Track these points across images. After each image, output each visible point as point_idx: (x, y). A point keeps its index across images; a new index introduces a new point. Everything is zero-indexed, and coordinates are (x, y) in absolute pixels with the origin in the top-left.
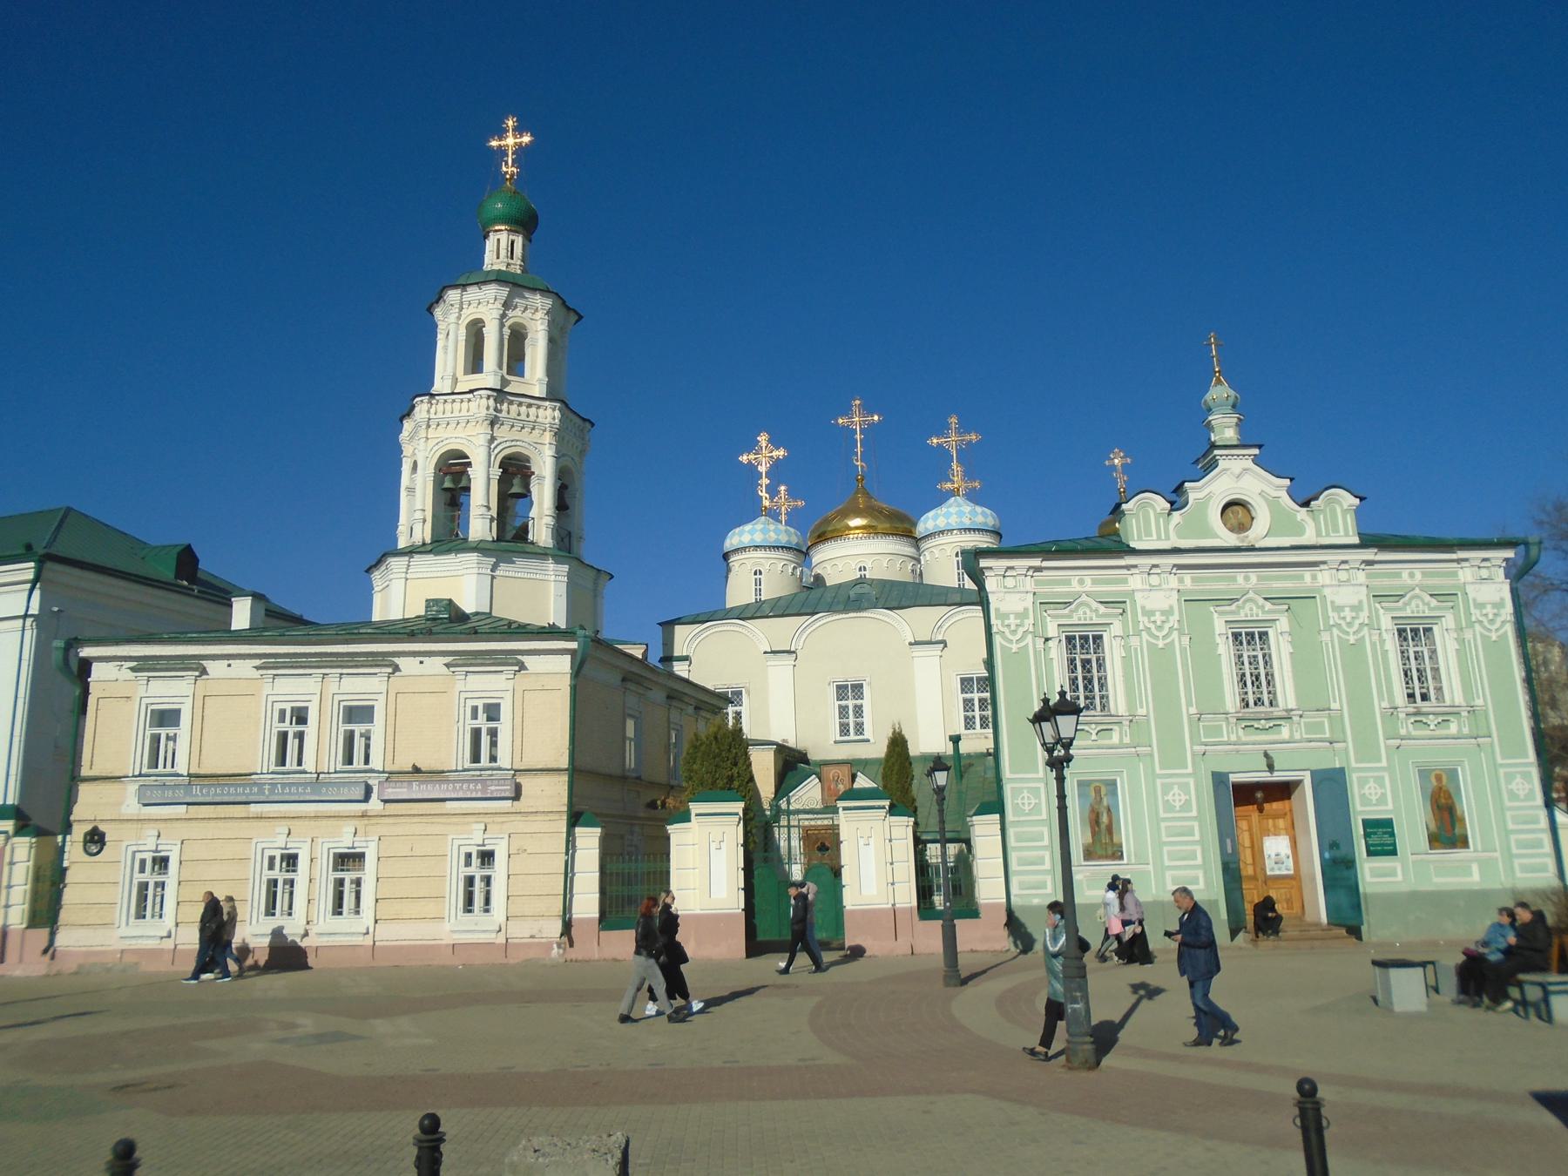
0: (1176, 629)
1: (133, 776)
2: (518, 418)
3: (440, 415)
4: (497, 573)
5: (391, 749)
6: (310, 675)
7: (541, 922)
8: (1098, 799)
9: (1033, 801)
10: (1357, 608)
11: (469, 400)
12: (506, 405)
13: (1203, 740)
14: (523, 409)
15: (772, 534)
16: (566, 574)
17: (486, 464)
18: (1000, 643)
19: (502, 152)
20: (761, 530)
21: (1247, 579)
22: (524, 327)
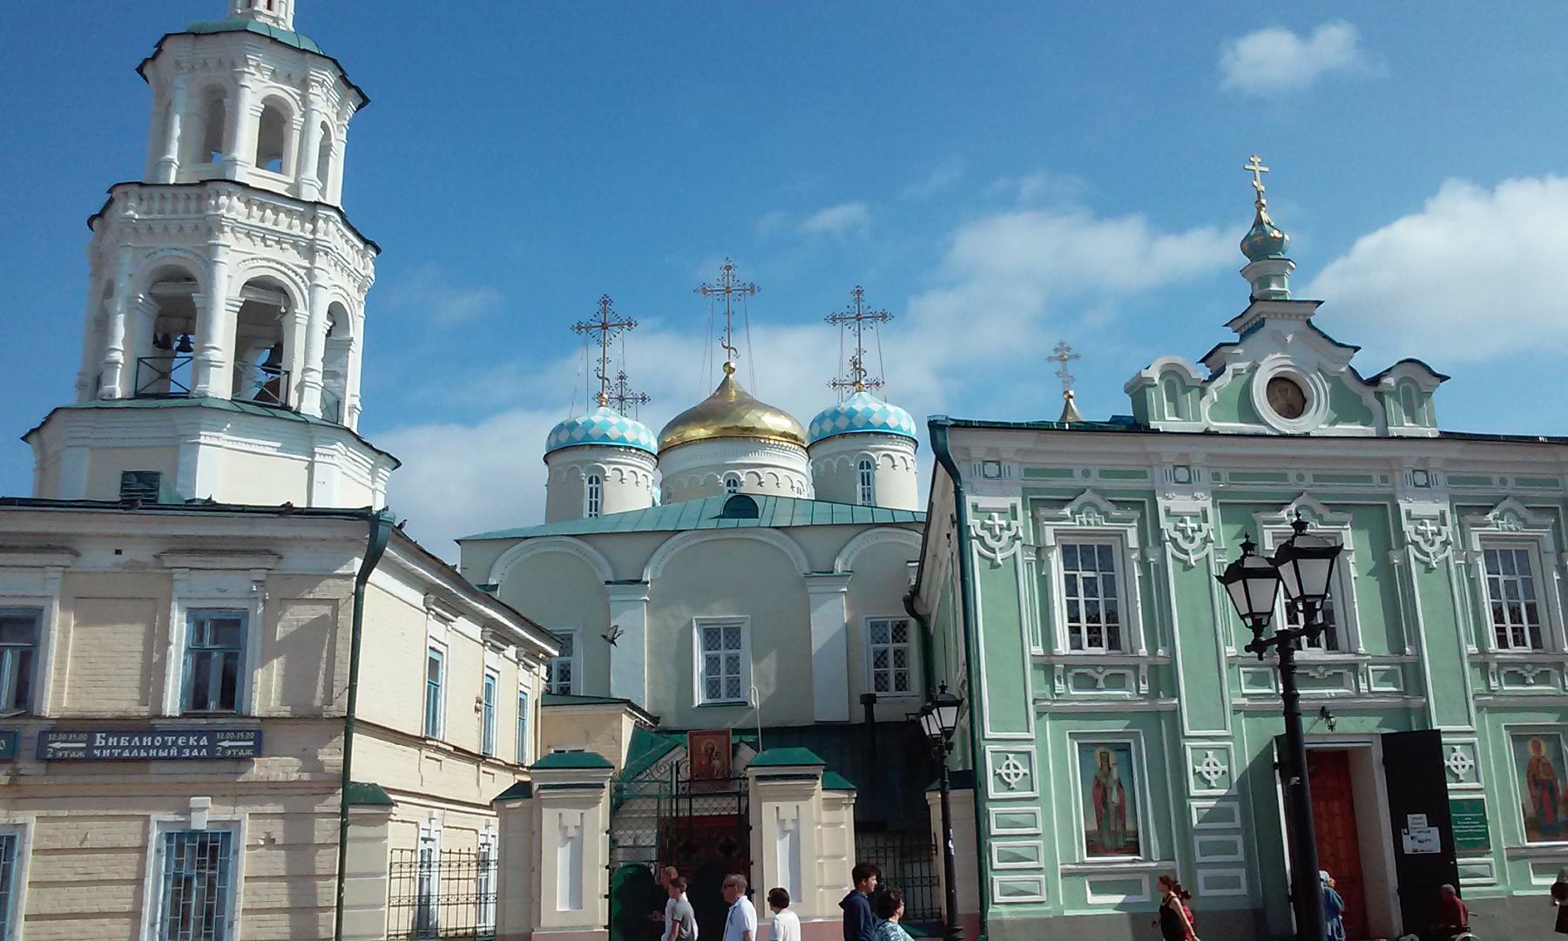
13: (1245, 691)
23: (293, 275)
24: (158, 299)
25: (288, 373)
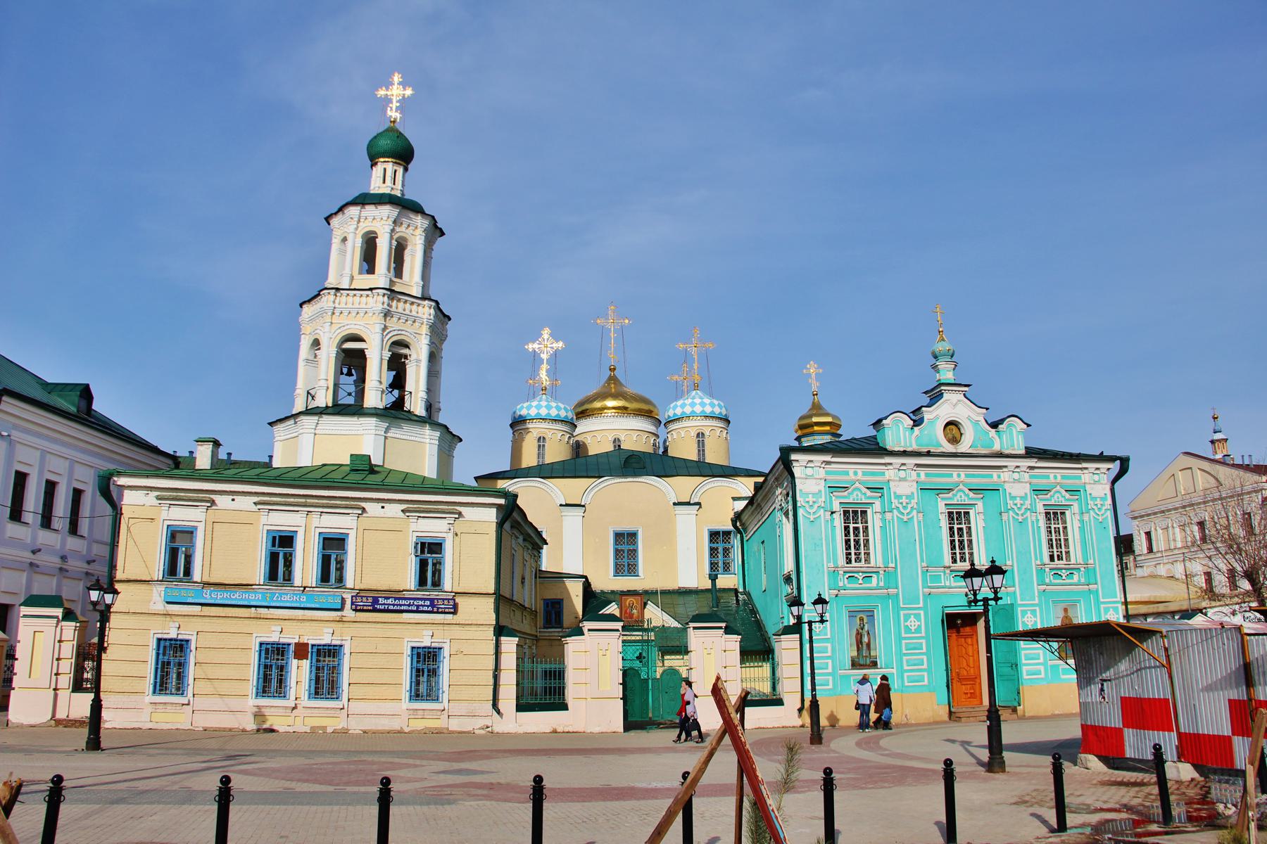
1: (157, 581)
2: (404, 313)
3: (343, 305)
4: (389, 435)
5: (360, 572)
6: (298, 511)
7: (474, 705)
8: (862, 625)
10: (1024, 498)
11: (368, 296)
12: (395, 301)
14: (408, 306)
15: (554, 409)
16: (438, 438)
17: (380, 347)
18: (803, 515)
19: (387, 100)
20: (546, 407)
21: (959, 476)
22: (405, 239)
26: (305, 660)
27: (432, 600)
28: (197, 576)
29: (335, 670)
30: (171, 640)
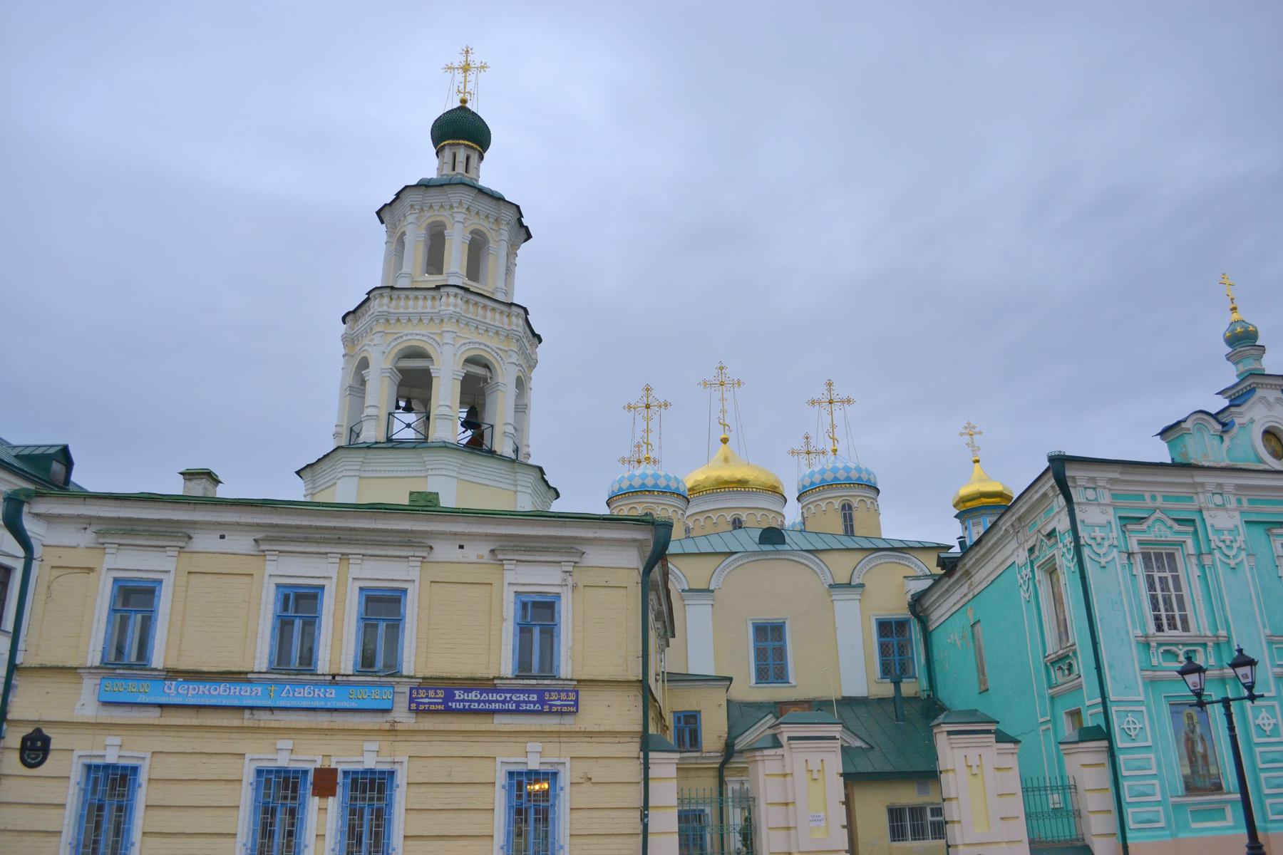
0: (1244, 550)
6: (326, 553)
8: (1191, 726)
9: (1138, 726)
23: (495, 355)
24: (401, 371)
25: (492, 426)
26: (331, 799)
27: (541, 693)
28: (158, 659)
29: (381, 817)
30: (106, 767)
